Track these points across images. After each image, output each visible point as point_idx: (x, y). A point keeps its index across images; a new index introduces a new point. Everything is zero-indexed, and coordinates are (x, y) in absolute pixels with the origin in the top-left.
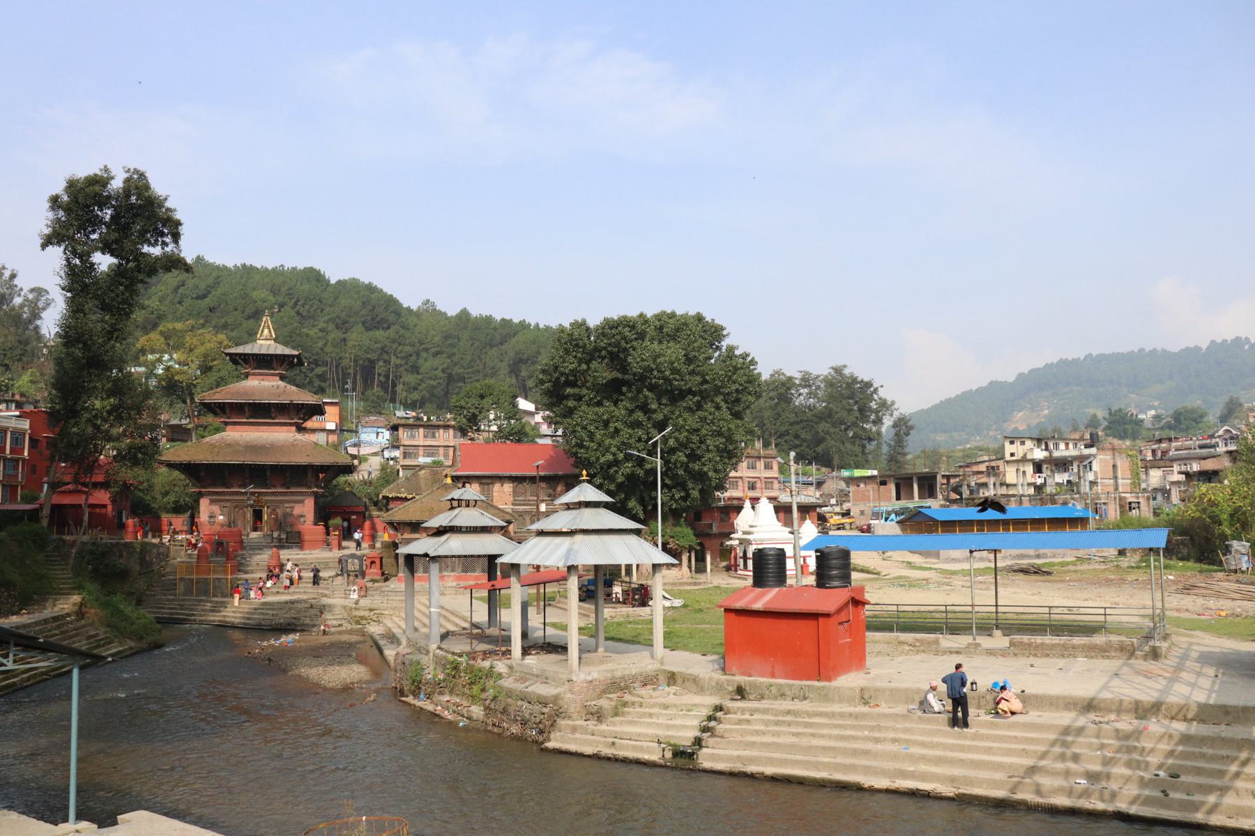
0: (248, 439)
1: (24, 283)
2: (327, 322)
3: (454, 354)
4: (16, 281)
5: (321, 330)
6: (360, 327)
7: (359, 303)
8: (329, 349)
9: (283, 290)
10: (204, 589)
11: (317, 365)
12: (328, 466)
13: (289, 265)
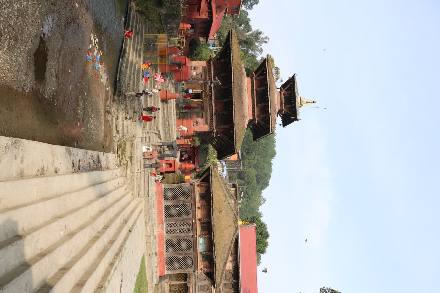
0: (244, 89)
1: (264, 46)
2: (258, 160)
3: (246, 213)
4: (264, 44)
5: (254, 157)
6: (256, 173)
7: (266, 172)
8: (247, 160)
9: (269, 142)
10: (149, 46)
11: (247, 153)
12: (233, 137)
13: (276, 144)
